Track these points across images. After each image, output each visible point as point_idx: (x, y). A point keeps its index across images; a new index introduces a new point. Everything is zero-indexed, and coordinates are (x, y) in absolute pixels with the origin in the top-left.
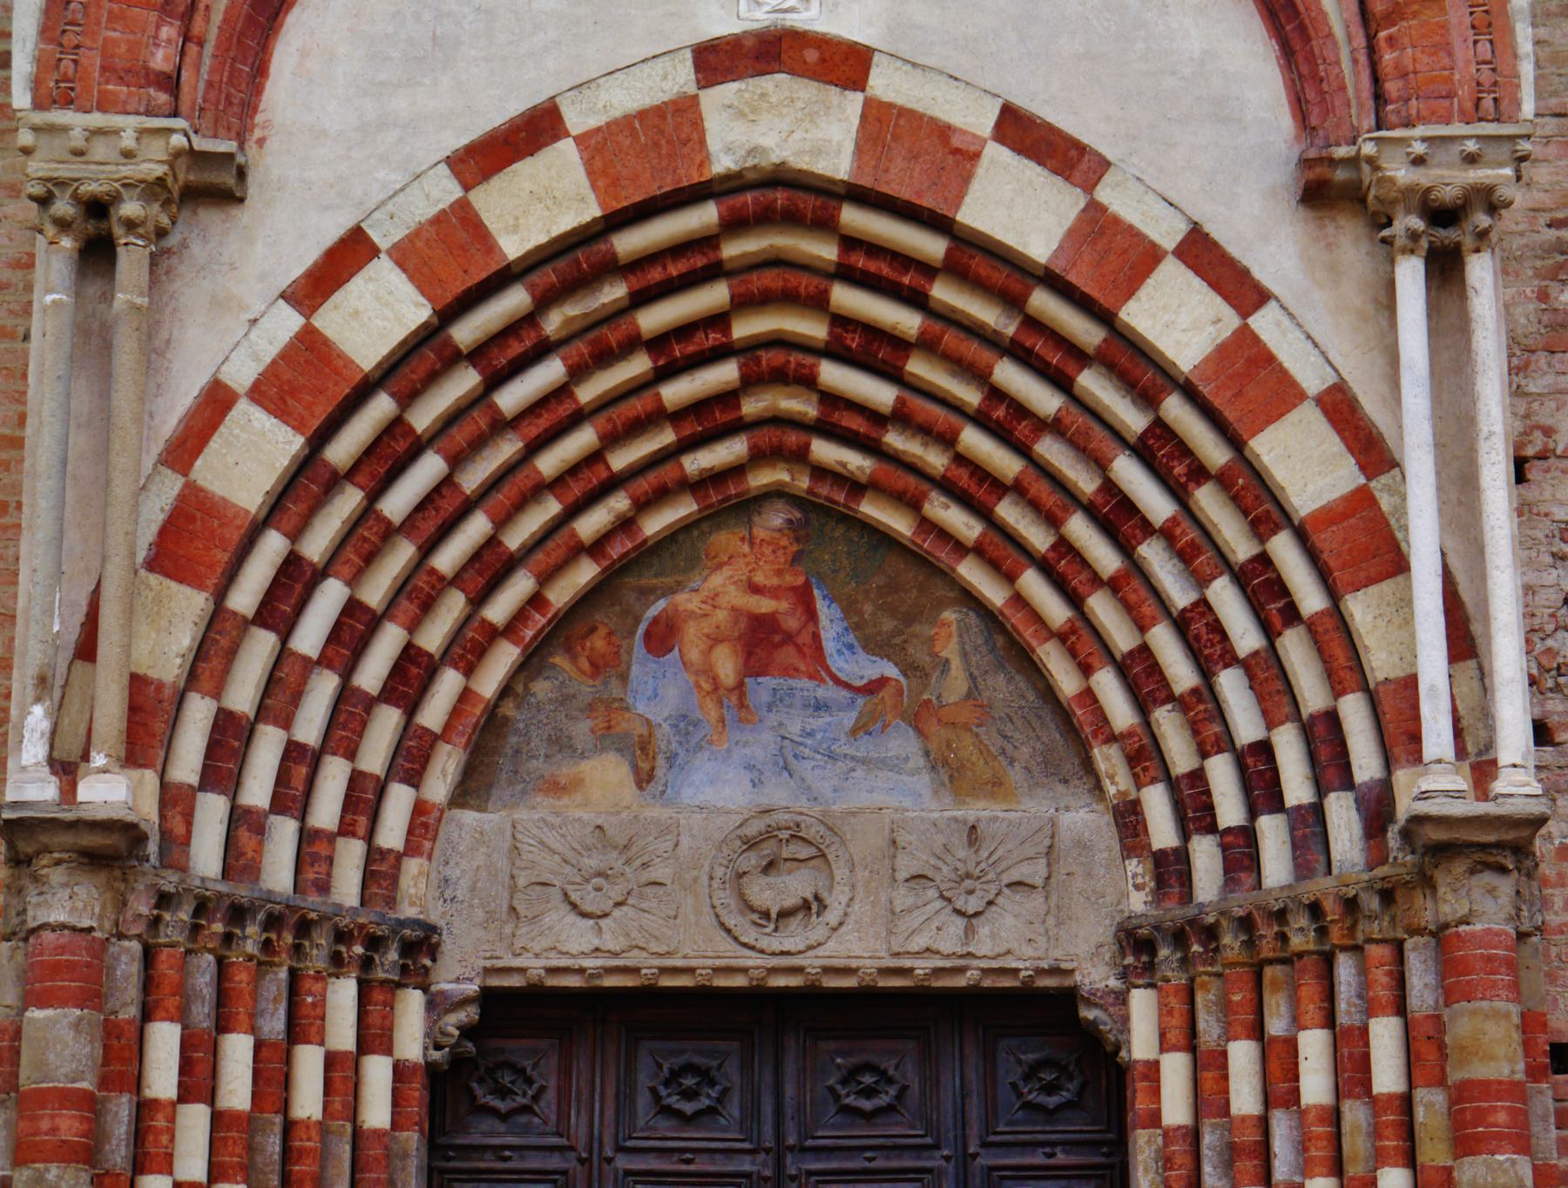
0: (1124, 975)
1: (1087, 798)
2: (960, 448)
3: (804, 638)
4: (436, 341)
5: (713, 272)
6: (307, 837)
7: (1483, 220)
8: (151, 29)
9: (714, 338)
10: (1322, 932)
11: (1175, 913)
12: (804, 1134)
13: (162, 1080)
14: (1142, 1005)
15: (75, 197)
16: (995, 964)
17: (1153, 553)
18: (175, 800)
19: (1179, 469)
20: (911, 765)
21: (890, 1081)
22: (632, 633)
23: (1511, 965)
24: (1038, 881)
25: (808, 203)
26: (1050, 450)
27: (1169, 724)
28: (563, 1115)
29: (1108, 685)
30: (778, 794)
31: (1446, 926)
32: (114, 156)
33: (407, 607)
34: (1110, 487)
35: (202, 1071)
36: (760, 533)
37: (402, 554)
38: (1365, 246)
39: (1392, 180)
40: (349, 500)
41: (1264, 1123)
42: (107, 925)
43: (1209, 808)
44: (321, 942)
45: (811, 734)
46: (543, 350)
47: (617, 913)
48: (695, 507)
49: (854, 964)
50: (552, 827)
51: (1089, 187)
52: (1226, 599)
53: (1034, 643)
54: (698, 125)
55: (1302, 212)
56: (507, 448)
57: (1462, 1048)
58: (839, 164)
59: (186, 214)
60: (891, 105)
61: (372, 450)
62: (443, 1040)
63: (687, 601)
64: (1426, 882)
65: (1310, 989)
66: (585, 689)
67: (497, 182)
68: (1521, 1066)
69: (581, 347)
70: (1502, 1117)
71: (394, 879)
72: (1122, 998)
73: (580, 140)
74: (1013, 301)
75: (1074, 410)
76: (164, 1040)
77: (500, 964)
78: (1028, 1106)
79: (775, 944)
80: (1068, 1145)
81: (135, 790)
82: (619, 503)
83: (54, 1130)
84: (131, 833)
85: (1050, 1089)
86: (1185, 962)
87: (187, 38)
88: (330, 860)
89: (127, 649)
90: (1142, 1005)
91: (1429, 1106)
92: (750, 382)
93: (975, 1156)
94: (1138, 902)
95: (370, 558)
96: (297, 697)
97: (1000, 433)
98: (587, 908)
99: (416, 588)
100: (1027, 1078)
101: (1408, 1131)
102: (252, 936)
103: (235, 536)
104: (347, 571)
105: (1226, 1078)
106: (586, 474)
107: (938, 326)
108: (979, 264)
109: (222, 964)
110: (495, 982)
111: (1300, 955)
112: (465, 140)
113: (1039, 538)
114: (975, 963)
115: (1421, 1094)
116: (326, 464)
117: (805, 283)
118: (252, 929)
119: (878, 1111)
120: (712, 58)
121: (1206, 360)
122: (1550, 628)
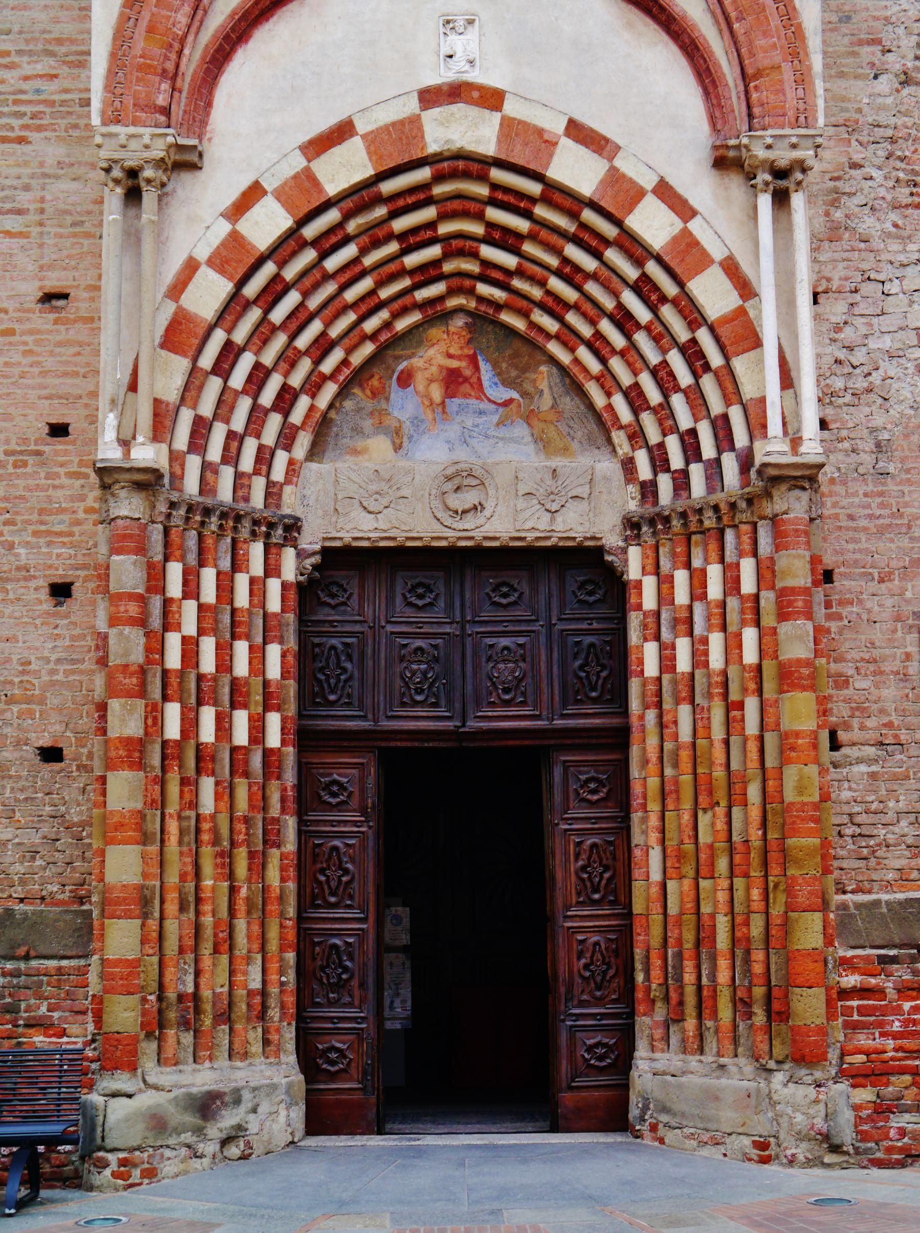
0: (626, 540)
1: (609, 456)
2: (548, 287)
3: (474, 380)
4: (296, 236)
5: (429, 201)
6: (238, 476)
7: (799, 176)
8: (157, 86)
9: (429, 234)
10: (719, 519)
11: (649, 510)
12: (473, 616)
13: (175, 589)
14: (634, 555)
15: (122, 168)
16: (565, 535)
17: (641, 338)
18: (176, 458)
19: (654, 297)
20: (525, 440)
21: (515, 590)
22: (391, 378)
23: (806, 533)
24: (585, 496)
25: (475, 167)
26: (591, 288)
27: (648, 420)
28: (361, 606)
29: (619, 403)
30: (462, 455)
31: (777, 515)
32: (140, 147)
33: (283, 366)
34: (620, 306)
35: (193, 585)
36: (452, 329)
37: (280, 340)
38: (743, 189)
39: (756, 156)
40: (255, 314)
41: (690, 608)
42: (147, 517)
43: (667, 461)
44: (247, 524)
45: (477, 426)
46: (347, 240)
47: (385, 511)
48: (420, 316)
49: (498, 535)
50: (354, 471)
51: (611, 159)
52: (676, 360)
53: (584, 381)
54: (420, 129)
55: (714, 172)
56: (330, 288)
57: (783, 572)
58: (488, 147)
59: (174, 175)
60: (514, 119)
61: (265, 290)
62: (304, 571)
63: (417, 362)
64: (768, 495)
65: (713, 546)
66: (369, 405)
67: (324, 157)
68: (809, 580)
69: (365, 239)
70: (800, 604)
71: (280, 495)
72: (624, 551)
73: (364, 137)
74: (574, 215)
75: (603, 268)
76: (175, 571)
77: (330, 536)
78: (580, 601)
79: (461, 527)
80: (599, 619)
81: (157, 453)
82: (384, 314)
83: (127, 611)
84: (157, 473)
85: (590, 593)
86: (654, 534)
87: (173, 89)
88: (250, 486)
89: (152, 386)
90: (634, 555)
91: (767, 599)
92: (448, 255)
93: (555, 625)
94: (633, 506)
95: (265, 342)
96: (232, 408)
97: (568, 280)
98: (371, 509)
99: (287, 357)
100: (579, 588)
101: (757, 611)
102: (214, 522)
103: (201, 332)
104: (254, 348)
105: (673, 587)
106: (368, 300)
107: (537, 227)
108: (557, 197)
109: (201, 537)
110: (328, 544)
111: (709, 530)
112: (308, 137)
113: (586, 331)
114: (555, 534)
115: (763, 594)
116: (244, 297)
117: (473, 207)
118: (214, 519)
119: (510, 604)
120: (427, 96)
121: (667, 244)
122: (828, 374)
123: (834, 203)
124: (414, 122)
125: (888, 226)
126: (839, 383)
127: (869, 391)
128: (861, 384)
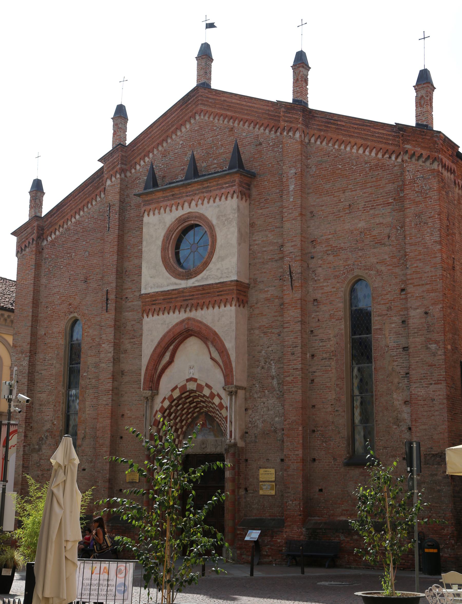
51: (211, 389)
82: (191, 414)
123: (251, 392)
124: (185, 385)
125: (259, 396)
126: (250, 425)
127: (254, 427)
128: (253, 425)
